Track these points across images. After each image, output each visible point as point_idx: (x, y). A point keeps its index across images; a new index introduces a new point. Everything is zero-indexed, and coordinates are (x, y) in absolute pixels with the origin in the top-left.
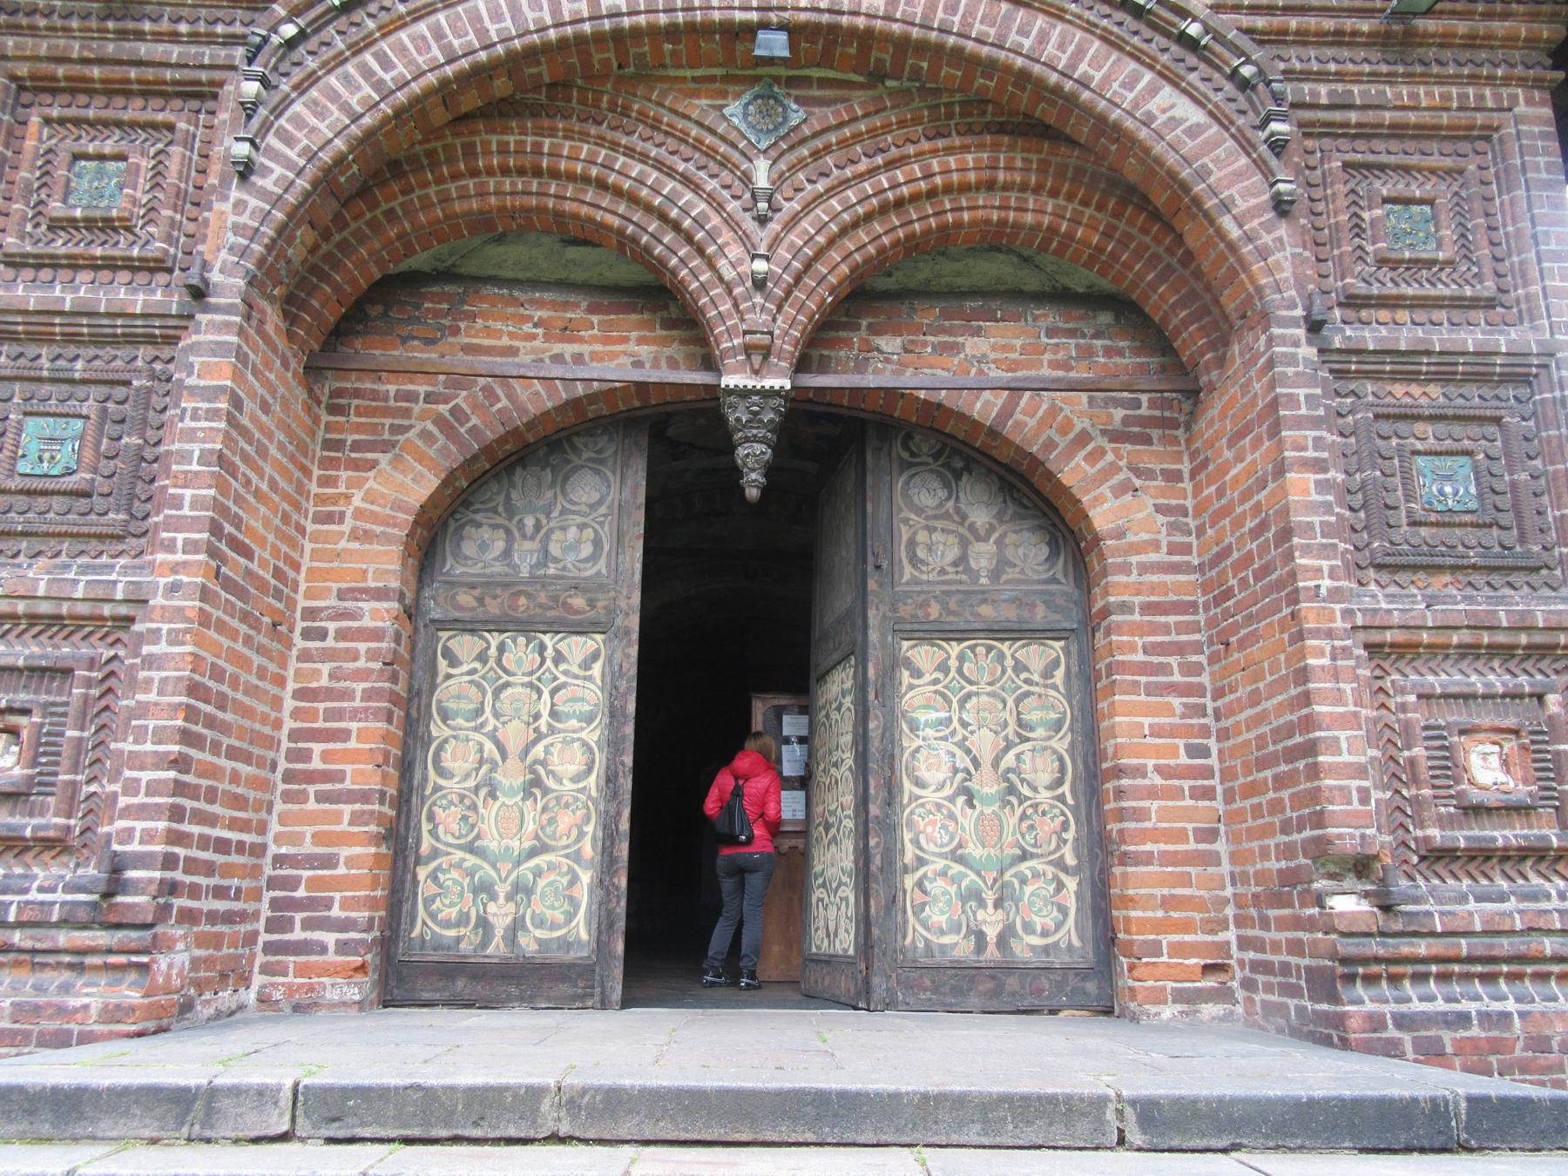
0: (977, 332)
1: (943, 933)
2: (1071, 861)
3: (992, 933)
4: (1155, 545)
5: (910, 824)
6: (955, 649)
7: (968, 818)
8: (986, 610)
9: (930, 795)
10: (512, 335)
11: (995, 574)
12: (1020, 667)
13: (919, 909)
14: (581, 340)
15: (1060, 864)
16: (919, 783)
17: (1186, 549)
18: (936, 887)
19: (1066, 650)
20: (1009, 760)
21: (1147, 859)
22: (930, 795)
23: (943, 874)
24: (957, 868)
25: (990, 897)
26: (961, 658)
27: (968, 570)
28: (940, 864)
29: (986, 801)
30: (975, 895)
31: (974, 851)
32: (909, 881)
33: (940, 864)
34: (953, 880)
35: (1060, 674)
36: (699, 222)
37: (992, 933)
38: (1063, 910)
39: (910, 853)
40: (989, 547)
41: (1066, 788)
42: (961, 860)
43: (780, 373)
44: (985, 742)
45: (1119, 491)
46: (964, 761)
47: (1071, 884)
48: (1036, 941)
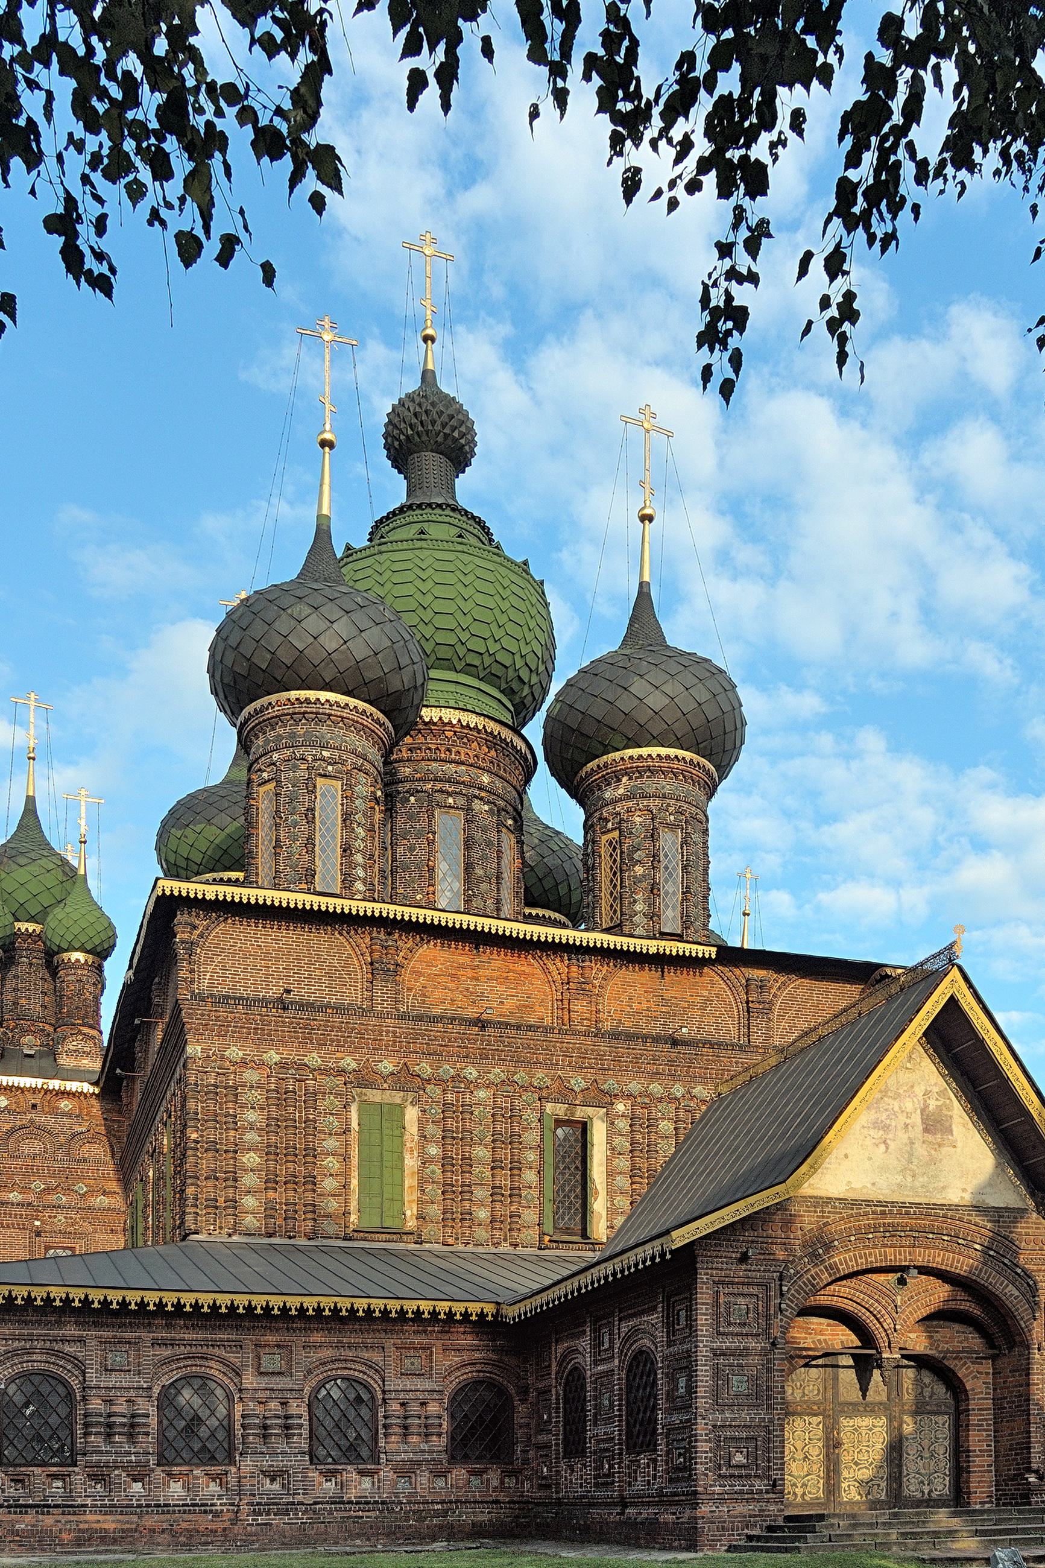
0: (937, 1332)
4: (982, 1393)
5: (906, 1465)
7: (921, 1463)
8: (928, 1407)
9: (910, 1457)
10: (806, 1333)
11: (930, 1397)
12: (936, 1423)
13: (907, 1487)
14: (825, 1335)
16: (909, 1455)
17: (989, 1394)
18: (912, 1481)
19: (949, 1418)
20: (932, 1448)
22: (910, 1457)
24: (918, 1476)
25: (926, 1483)
26: (920, 1420)
27: (923, 1396)
29: (926, 1458)
30: (922, 1482)
31: (922, 1471)
32: (905, 1479)
34: (917, 1479)
35: (947, 1425)
36: (879, 1312)
39: (905, 1473)
40: (929, 1389)
41: (947, 1455)
42: (919, 1474)
43: (896, 1353)
44: (925, 1444)
45: (973, 1378)
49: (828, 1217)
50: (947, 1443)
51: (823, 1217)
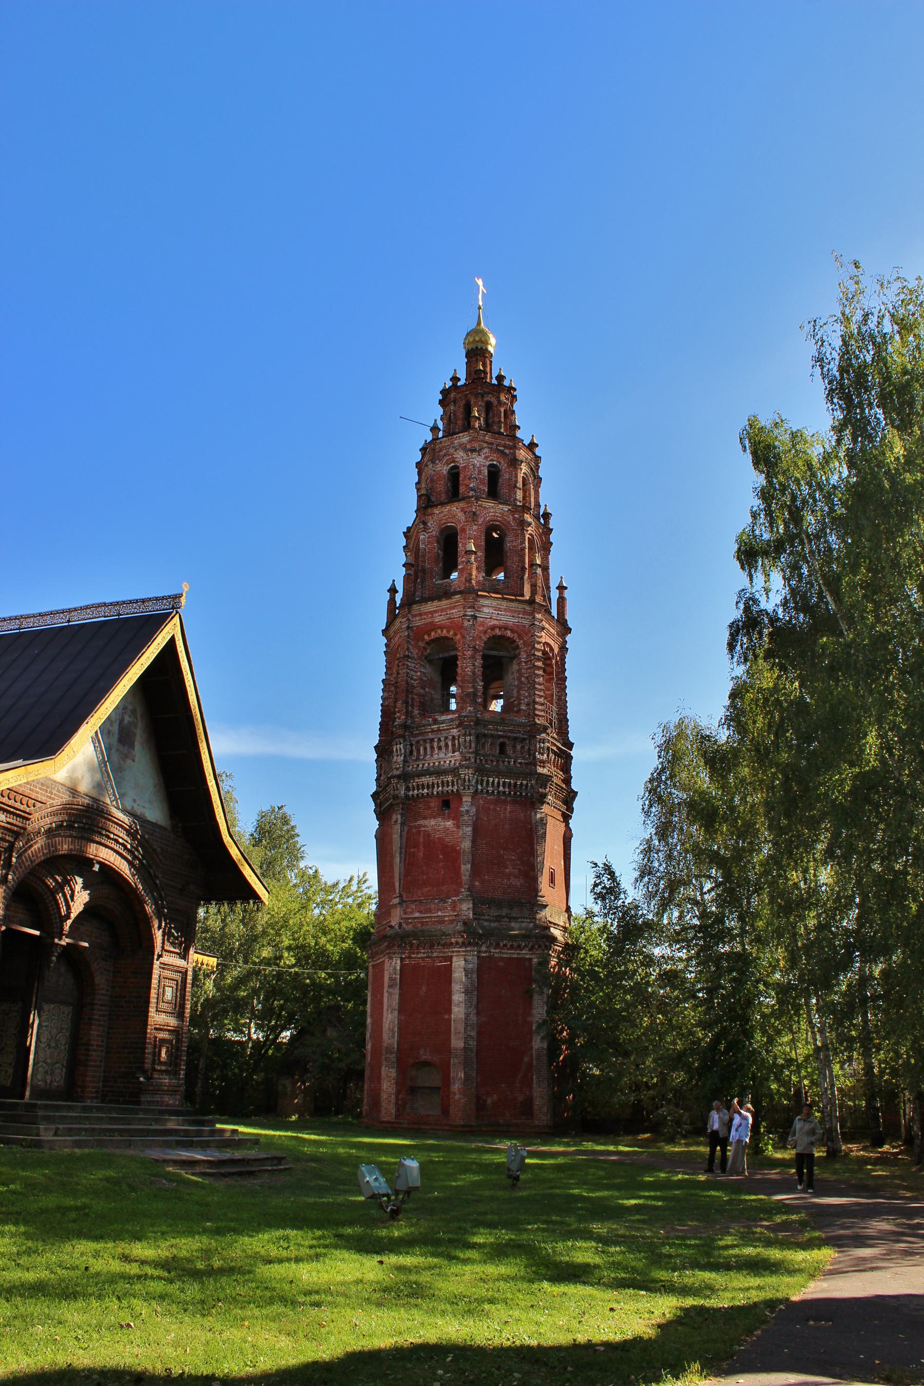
1: (39, 1081)
2: (65, 1064)
3: (49, 1081)
6: (52, 1006)
15: (63, 1065)
21: (91, 1066)
23: (41, 1066)
24: (45, 1065)
25: (49, 1072)
28: (41, 1063)
31: (49, 1061)
33: (41, 1063)
35: (70, 1015)
37: (49, 1081)
38: (62, 1076)
44: (54, 1031)
46: (50, 1037)
47: (64, 1070)
48: (56, 1084)
49: (54, 799)
50: (68, 1034)
51: (50, 798)
